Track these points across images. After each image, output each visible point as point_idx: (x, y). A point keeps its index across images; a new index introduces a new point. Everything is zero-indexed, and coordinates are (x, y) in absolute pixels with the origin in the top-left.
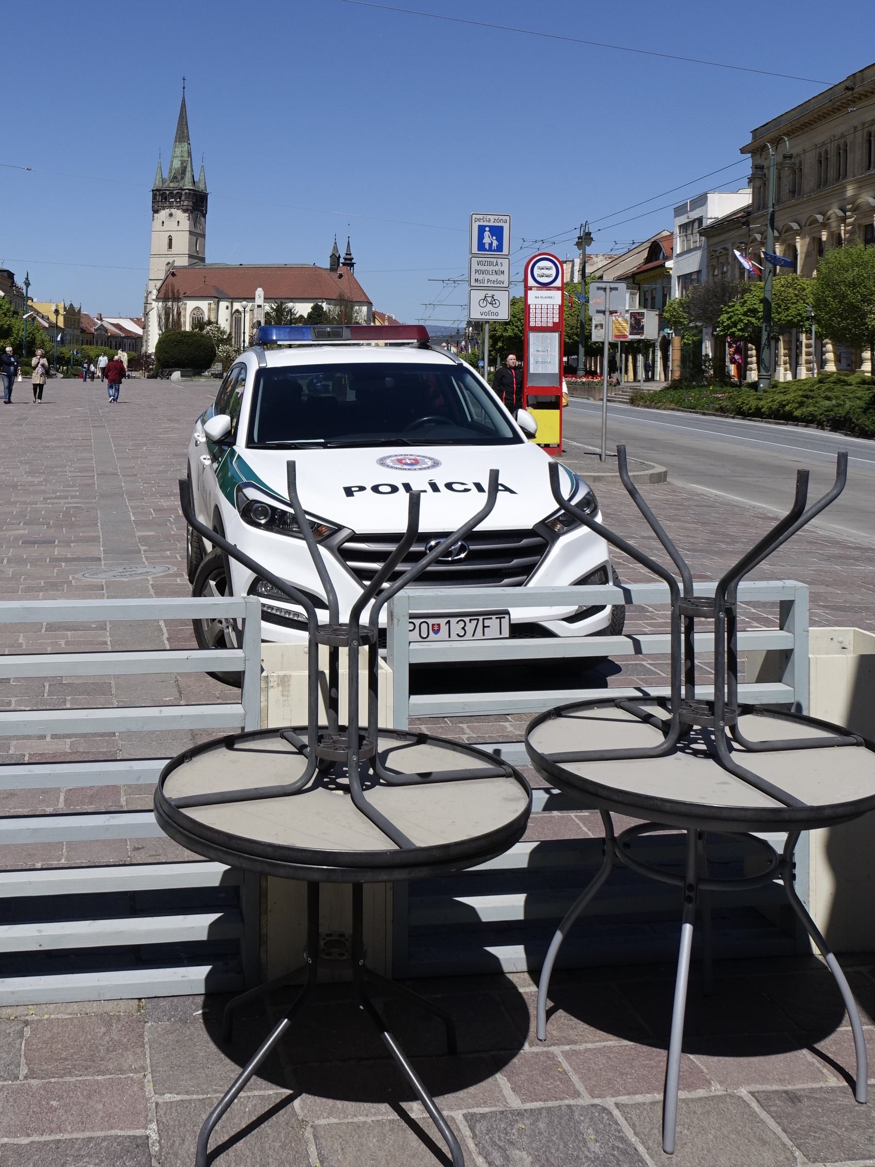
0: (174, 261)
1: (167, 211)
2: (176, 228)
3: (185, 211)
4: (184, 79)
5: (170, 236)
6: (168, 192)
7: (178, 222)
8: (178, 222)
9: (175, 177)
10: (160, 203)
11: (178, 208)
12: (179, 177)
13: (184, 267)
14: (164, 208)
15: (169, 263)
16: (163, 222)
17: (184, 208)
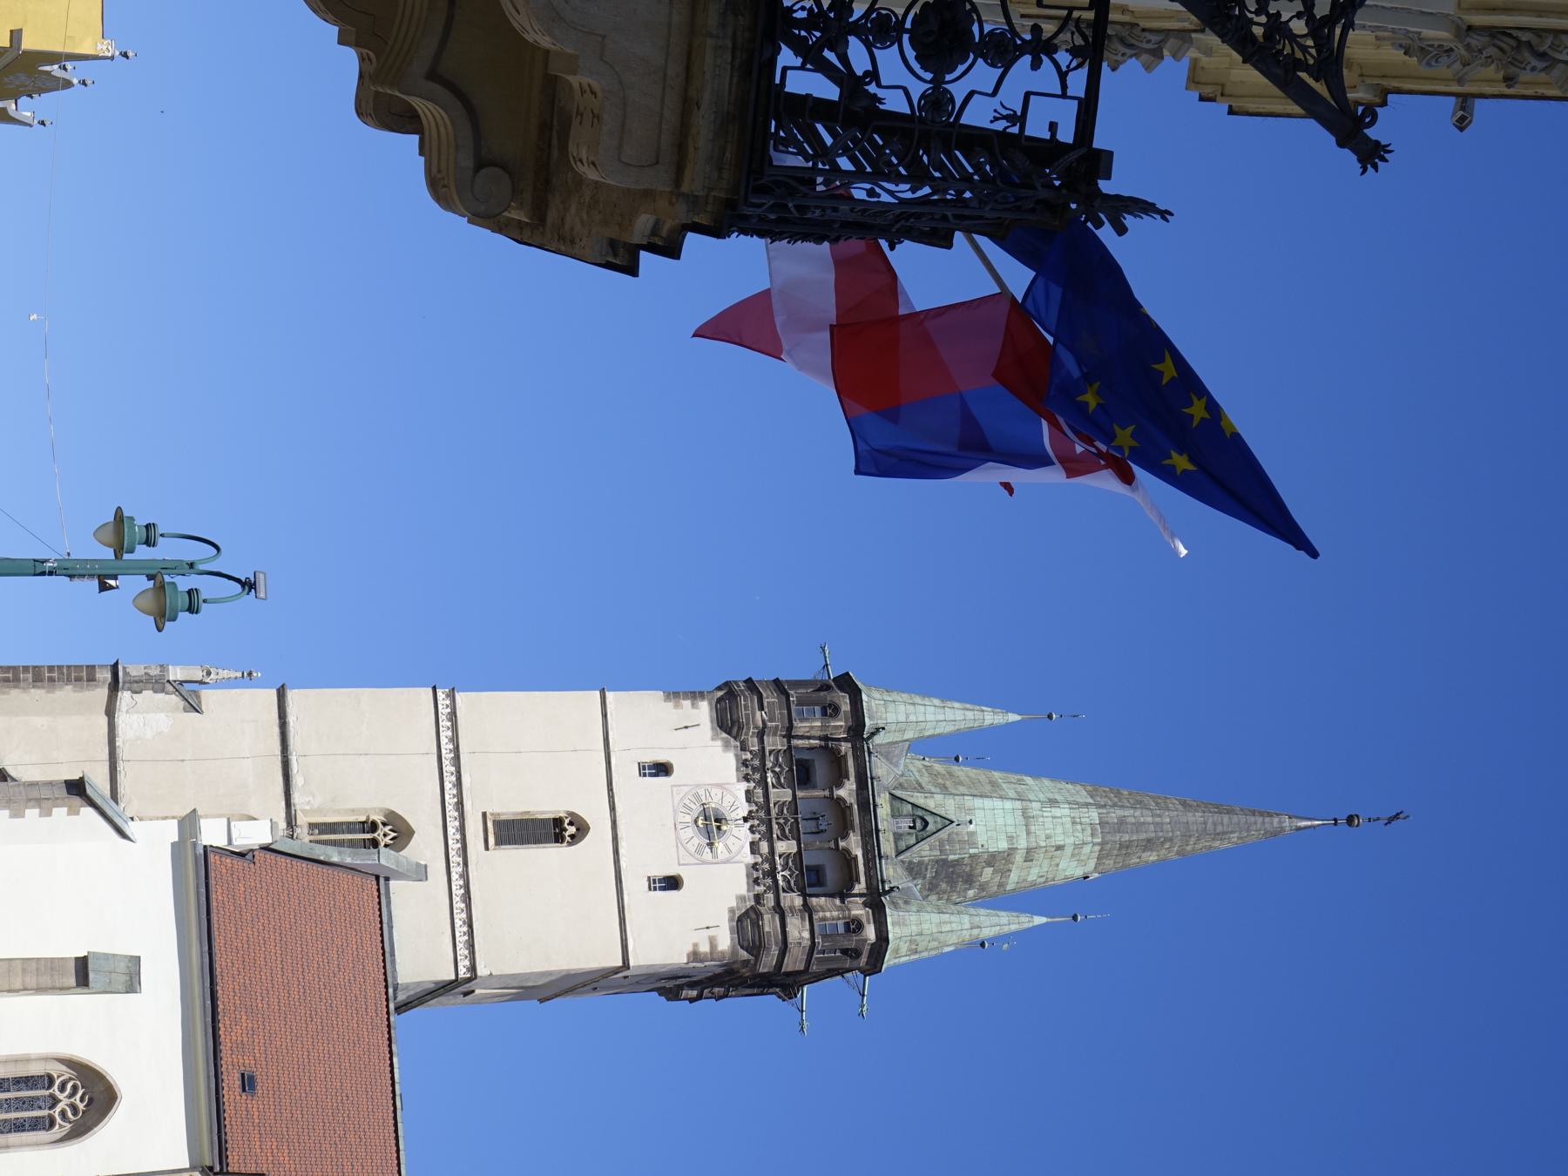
0: (421, 873)
1: (734, 799)
2: (642, 863)
3: (747, 921)
4: (1390, 820)
5: (582, 829)
6: (847, 791)
7: (672, 883)
8: (672, 883)
9: (922, 823)
10: (774, 743)
11: (761, 873)
12: (925, 851)
13: (386, 955)
14: (752, 770)
15: (402, 833)
16: (662, 769)
17: (770, 924)
